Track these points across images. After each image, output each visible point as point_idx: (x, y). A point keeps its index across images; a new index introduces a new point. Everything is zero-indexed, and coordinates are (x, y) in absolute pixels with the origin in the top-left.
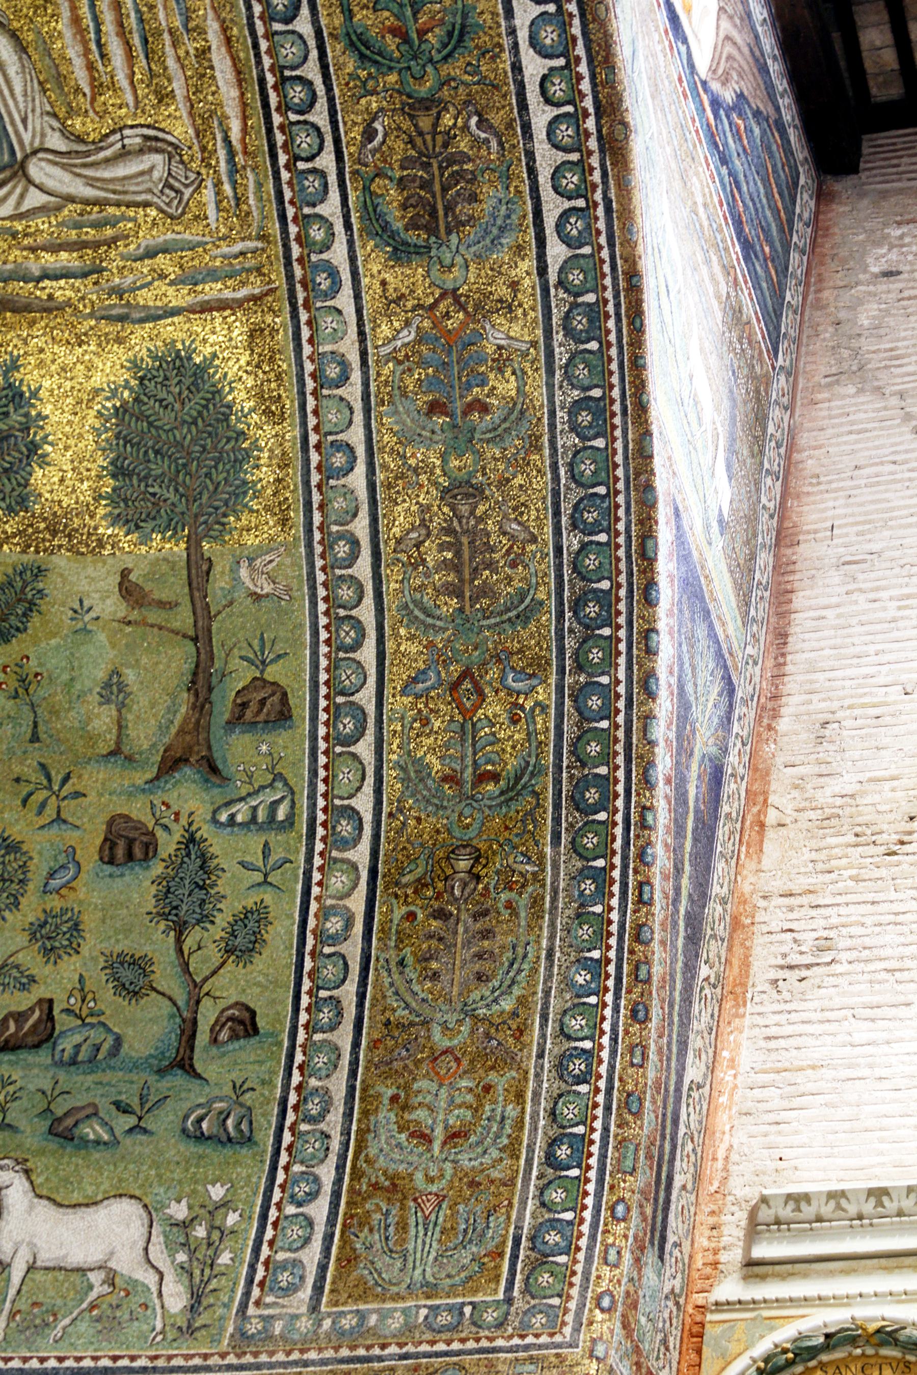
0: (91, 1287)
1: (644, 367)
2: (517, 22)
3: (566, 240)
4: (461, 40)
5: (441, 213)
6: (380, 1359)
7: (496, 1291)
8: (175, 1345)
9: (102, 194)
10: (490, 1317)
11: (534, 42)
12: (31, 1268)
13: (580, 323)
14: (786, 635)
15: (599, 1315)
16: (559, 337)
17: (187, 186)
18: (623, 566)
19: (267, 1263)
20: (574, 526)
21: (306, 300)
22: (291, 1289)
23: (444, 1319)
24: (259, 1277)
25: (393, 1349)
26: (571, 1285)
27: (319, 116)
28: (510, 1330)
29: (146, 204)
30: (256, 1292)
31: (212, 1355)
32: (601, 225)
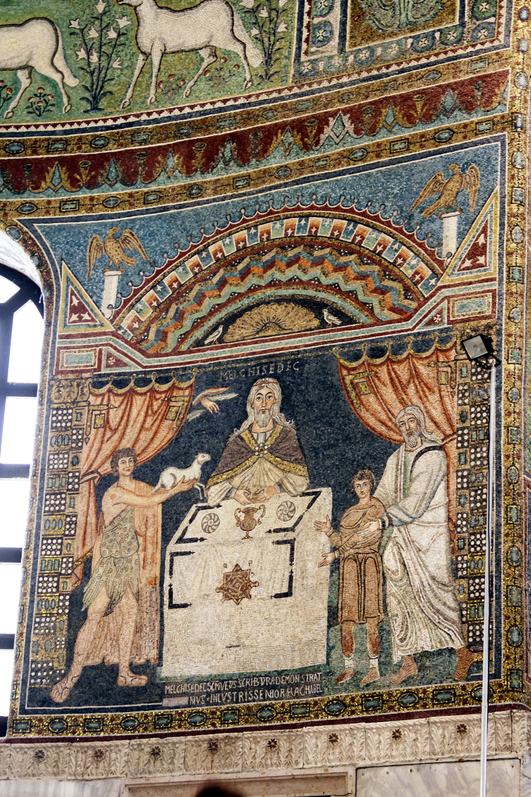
0: (202, 60)
6: (387, 75)
7: (453, 20)
8: (260, 87)
10: (452, 37)
12: (164, 54)
15: (520, 24)
19: (308, 27)
22: (326, 40)
23: (424, 43)
24: (304, 37)
25: (394, 68)
26: (501, 7)
28: (465, 43)
30: (304, 46)
31: (284, 89)
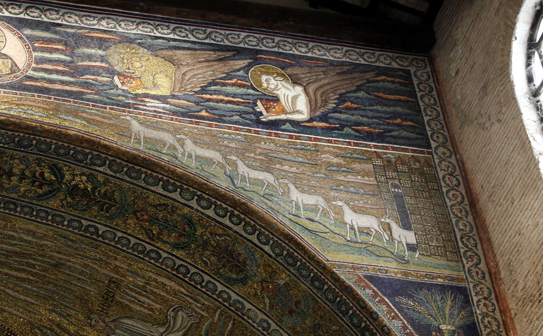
1: (314, 256)
2: (195, 207)
3: (265, 244)
4: (192, 224)
5: (239, 264)
9: (183, 331)
11: (204, 208)
13: (290, 261)
14: (490, 239)
16: (291, 269)
17: (192, 313)
18: (361, 315)
20: (343, 314)
21: (242, 313)
27: (193, 270)
29: (192, 324)
32: (267, 233)
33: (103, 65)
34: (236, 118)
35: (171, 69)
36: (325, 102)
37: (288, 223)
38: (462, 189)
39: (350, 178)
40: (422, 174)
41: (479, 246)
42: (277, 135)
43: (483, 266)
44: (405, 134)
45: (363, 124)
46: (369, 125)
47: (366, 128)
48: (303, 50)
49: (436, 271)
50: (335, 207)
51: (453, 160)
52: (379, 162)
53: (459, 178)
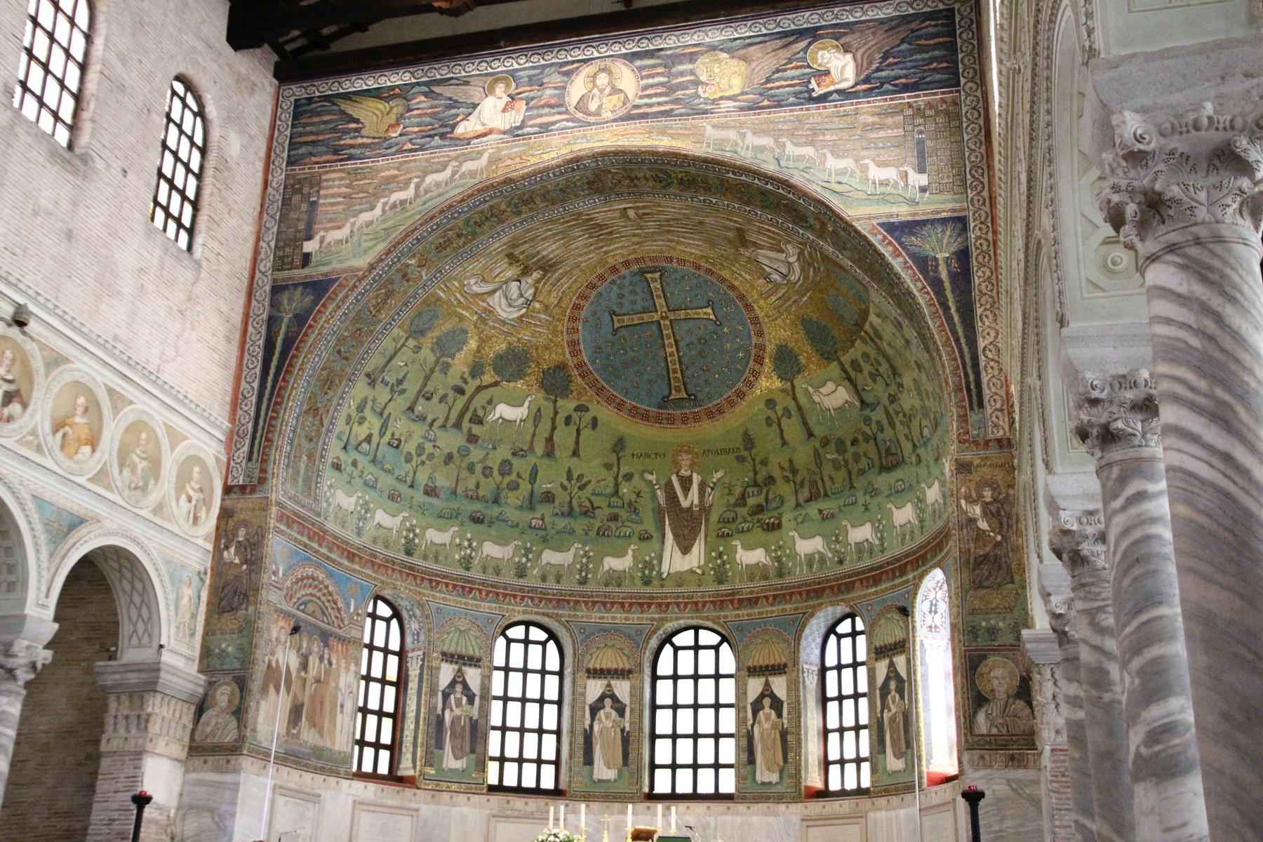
33: (692, 78)
34: (792, 99)
35: (742, 66)
36: (870, 63)
37: (819, 190)
38: (981, 122)
39: (882, 134)
40: (947, 113)
41: (986, 175)
42: (825, 108)
43: (985, 194)
44: (938, 77)
45: (900, 77)
46: (906, 77)
47: (903, 81)
48: (858, 15)
49: (943, 206)
50: (862, 165)
51: (979, 94)
52: (909, 112)
53: (981, 110)
